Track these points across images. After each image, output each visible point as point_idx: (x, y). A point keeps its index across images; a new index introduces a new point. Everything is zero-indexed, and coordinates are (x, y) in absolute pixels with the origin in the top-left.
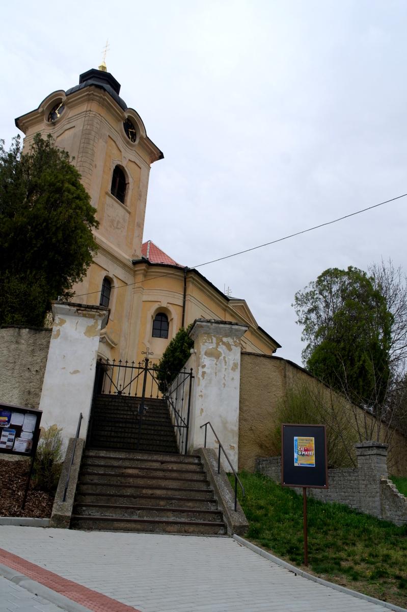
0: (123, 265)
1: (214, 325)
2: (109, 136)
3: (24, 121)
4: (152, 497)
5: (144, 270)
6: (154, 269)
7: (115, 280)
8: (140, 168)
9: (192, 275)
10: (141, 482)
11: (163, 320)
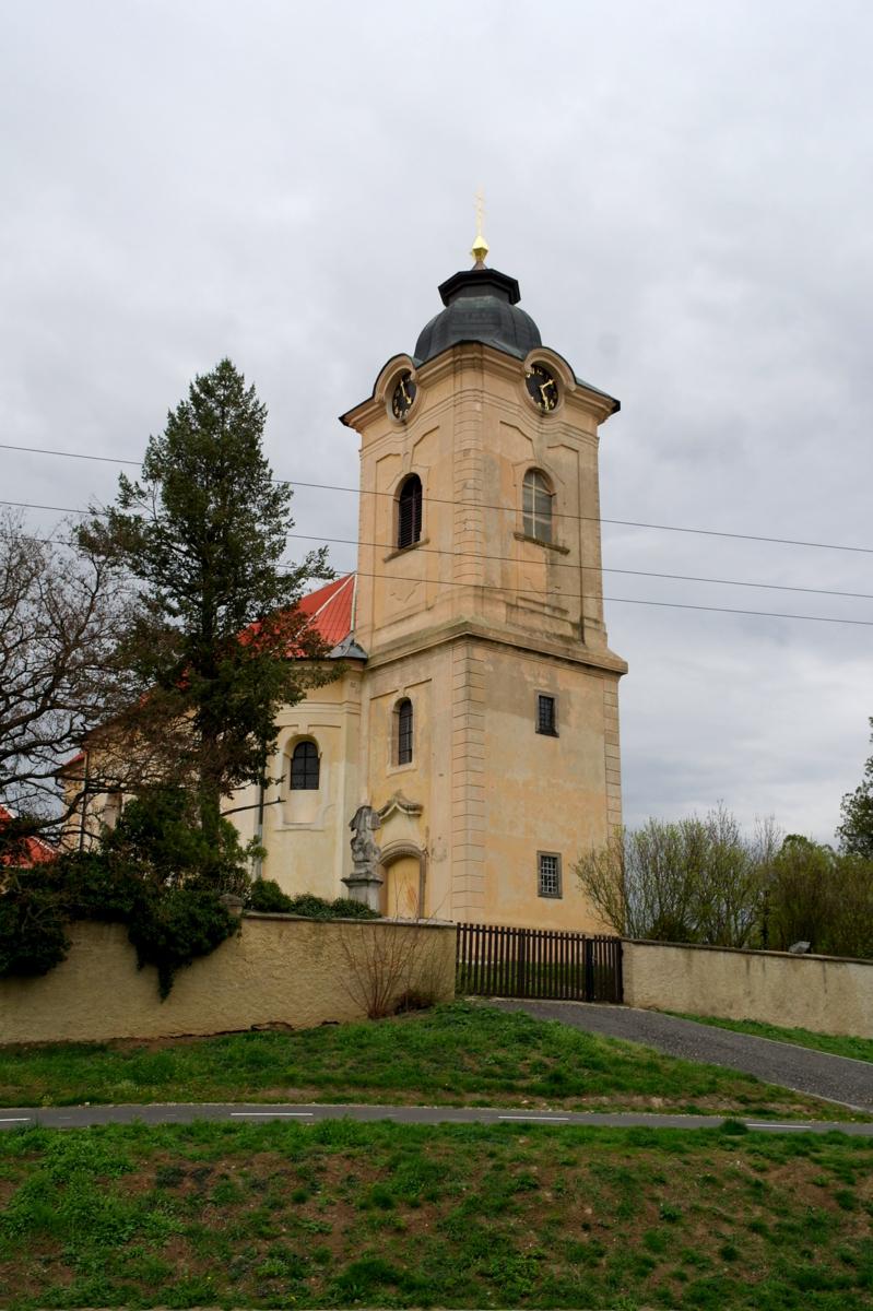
3: (355, 419)
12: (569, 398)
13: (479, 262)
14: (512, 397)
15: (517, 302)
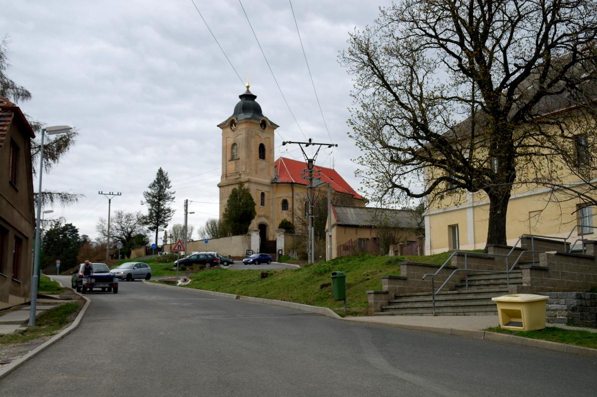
0: (268, 185)
6: (279, 185)
9: (295, 184)
13: (248, 91)
14: (257, 129)
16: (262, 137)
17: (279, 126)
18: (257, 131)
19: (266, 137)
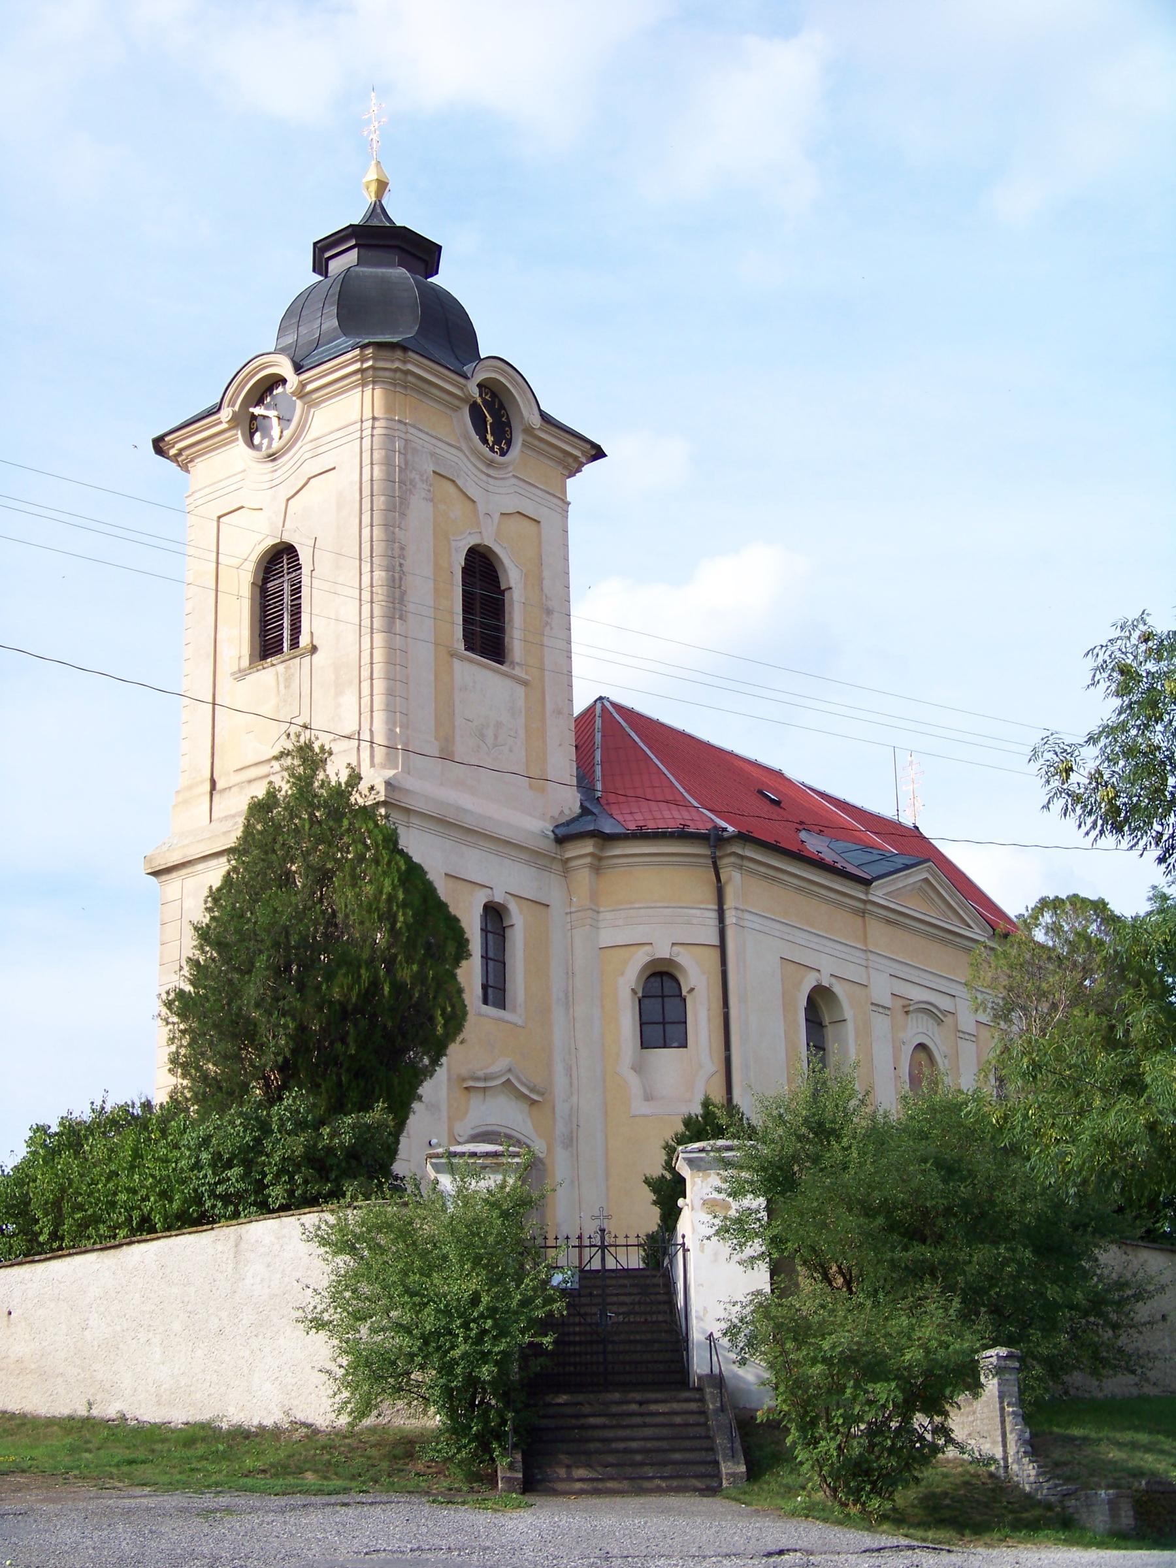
1: (712, 1154)
2: (434, 472)
4: (626, 1451)
5: (592, 854)
6: (619, 849)
7: (513, 906)
8: (539, 522)
10: (610, 1434)
11: (666, 992)
12: (530, 439)
15: (432, 276)
16: (491, 502)
17: (598, 453)
18: (449, 454)
19: (511, 504)
